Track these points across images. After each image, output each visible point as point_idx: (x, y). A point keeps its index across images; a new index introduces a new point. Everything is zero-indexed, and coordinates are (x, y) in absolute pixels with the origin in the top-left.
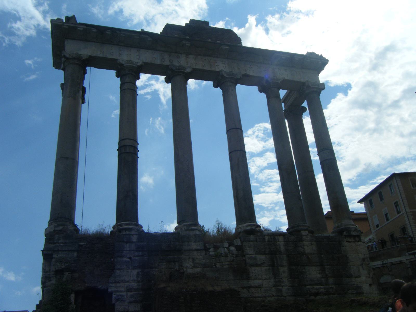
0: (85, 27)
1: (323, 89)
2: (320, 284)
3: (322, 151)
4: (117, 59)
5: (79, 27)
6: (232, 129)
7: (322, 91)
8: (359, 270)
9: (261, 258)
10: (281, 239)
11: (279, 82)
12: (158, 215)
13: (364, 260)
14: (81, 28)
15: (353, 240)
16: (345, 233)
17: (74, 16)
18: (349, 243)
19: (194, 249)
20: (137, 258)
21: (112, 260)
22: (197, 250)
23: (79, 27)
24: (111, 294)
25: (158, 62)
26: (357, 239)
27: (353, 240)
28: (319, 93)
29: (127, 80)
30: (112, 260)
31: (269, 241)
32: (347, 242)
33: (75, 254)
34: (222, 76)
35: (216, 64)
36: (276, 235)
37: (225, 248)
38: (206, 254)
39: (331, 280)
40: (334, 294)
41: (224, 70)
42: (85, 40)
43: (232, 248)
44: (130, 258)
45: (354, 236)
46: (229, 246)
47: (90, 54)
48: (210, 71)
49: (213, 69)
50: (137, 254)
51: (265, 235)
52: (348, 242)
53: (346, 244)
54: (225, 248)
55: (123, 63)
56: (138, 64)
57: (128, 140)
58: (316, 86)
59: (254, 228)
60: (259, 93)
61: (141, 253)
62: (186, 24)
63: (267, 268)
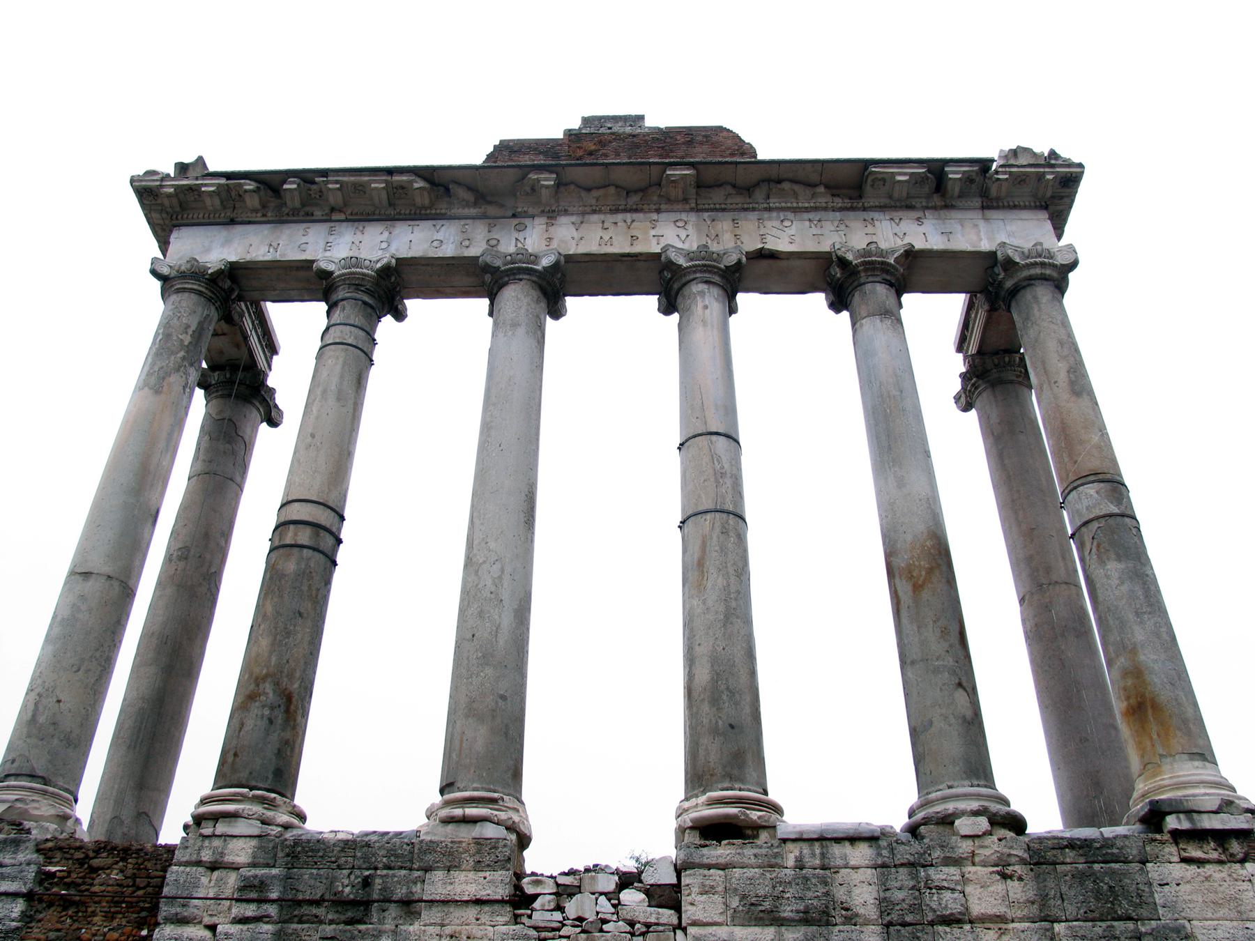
0: (223, 181)
1: (1073, 265)
3: (1075, 488)
4: (313, 261)
5: (206, 185)
6: (695, 437)
7: (1071, 275)
12: (369, 771)
14: (211, 185)
15: (1214, 855)
16: (1172, 822)
17: (200, 161)
18: (1193, 869)
19: (466, 898)
20: (235, 929)
21: (144, 933)
22: (479, 902)
23: (206, 185)
25: (449, 250)
27: (1214, 855)
28: (1060, 286)
29: (338, 316)
30: (144, 933)
31: (800, 866)
32: (1183, 865)
34: (670, 265)
35: (653, 232)
36: (838, 840)
37: (601, 894)
38: (516, 919)
41: (680, 245)
42: (232, 222)
44: (212, 928)
47: (233, 258)
48: (628, 255)
49: (638, 248)
50: (238, 910)
51: (784, 841)
52: (1185, 860)
53: (1178, 870)
54: (601, 894)
55: (331, 267)
56: (379, 265)
57: (296, 504)
58: (1038, 260)
60: (831, 313)
61: (250, 910)
62: (569, 133)
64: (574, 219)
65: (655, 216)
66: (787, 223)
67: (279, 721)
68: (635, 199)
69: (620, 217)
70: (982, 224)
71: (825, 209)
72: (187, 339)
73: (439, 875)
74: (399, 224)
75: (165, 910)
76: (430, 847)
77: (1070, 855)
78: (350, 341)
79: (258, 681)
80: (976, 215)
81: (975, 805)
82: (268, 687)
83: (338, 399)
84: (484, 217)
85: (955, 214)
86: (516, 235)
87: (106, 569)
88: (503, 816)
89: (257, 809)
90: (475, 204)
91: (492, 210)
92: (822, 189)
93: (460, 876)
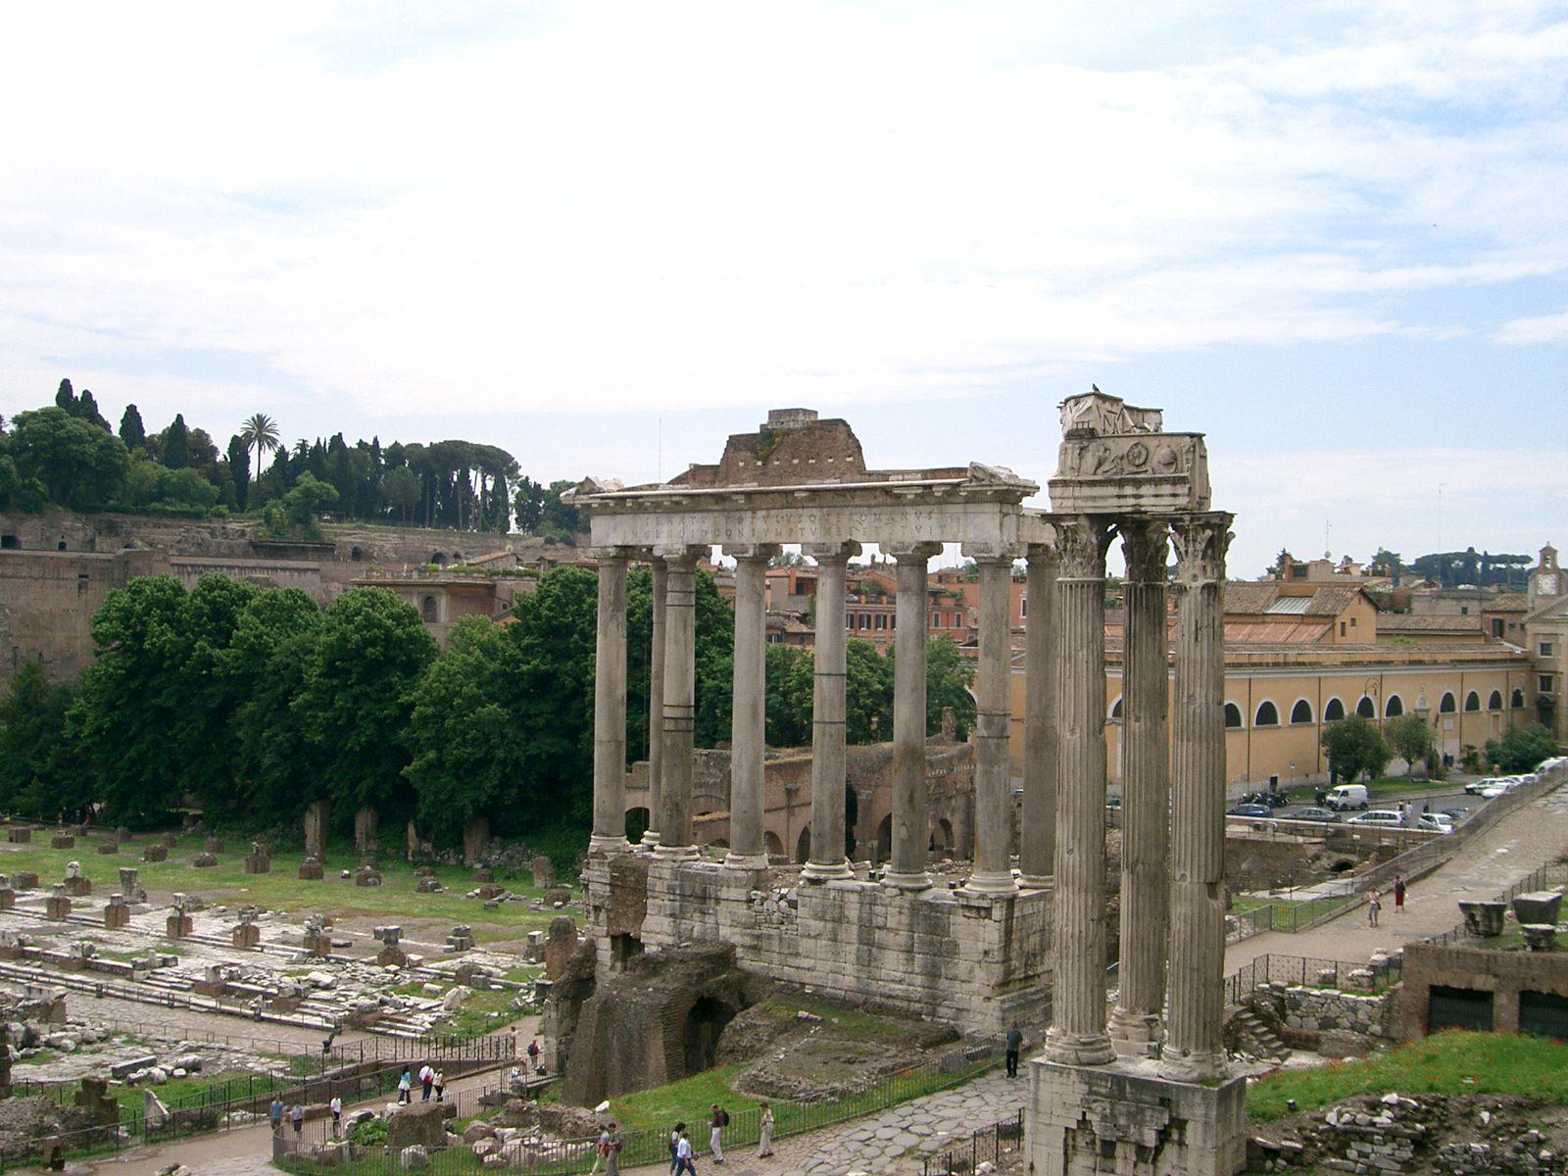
0: (599, 501)
2: (900, 982)
8: (971, 971)
9: (816, 926)
10: (854, 898)
11: (910, 552)
13: (986, 953)
24: (643, 945)
26: (983, 913)
31: (835, 899)
33: (608, 888)
35: (800, 526)
38: (749, 908)
39: (919, 980)
40: (919, 1002)
41: (811, 539)
43: (783, 903)
45: (978, 909)
46: (780, 899)
49: (793, 539)
53: (960, 919)
59: (812, 875)
61: (672, 897)
62: (762, 426)
63: (824, 942)
64: (764, 513)
65: (800, 511)
66: (863, 518)
67: (675, 815)
68: (790, 499)
69: (785, 511)
70: (962, 516)
71: (883, 505)
72: (612, 598)
73: (725, 888)
74: (686, 515)
75: (649, 894)
76: (722, 878)
77: (925, 907)
78: (676, 603)
79: (665, 798)
80: (959, 508)
81: (893, 884)
82: (668, 801)
83: (676, 642)
84: (725, 510)
85: (950, 508)
86: (737, 526)
87: (607, 738)
88: (744, 866)
89: (670, 856)
90: (717, 503)
91: (727, 505)
92: (878, 493)
93: (732, 890)
